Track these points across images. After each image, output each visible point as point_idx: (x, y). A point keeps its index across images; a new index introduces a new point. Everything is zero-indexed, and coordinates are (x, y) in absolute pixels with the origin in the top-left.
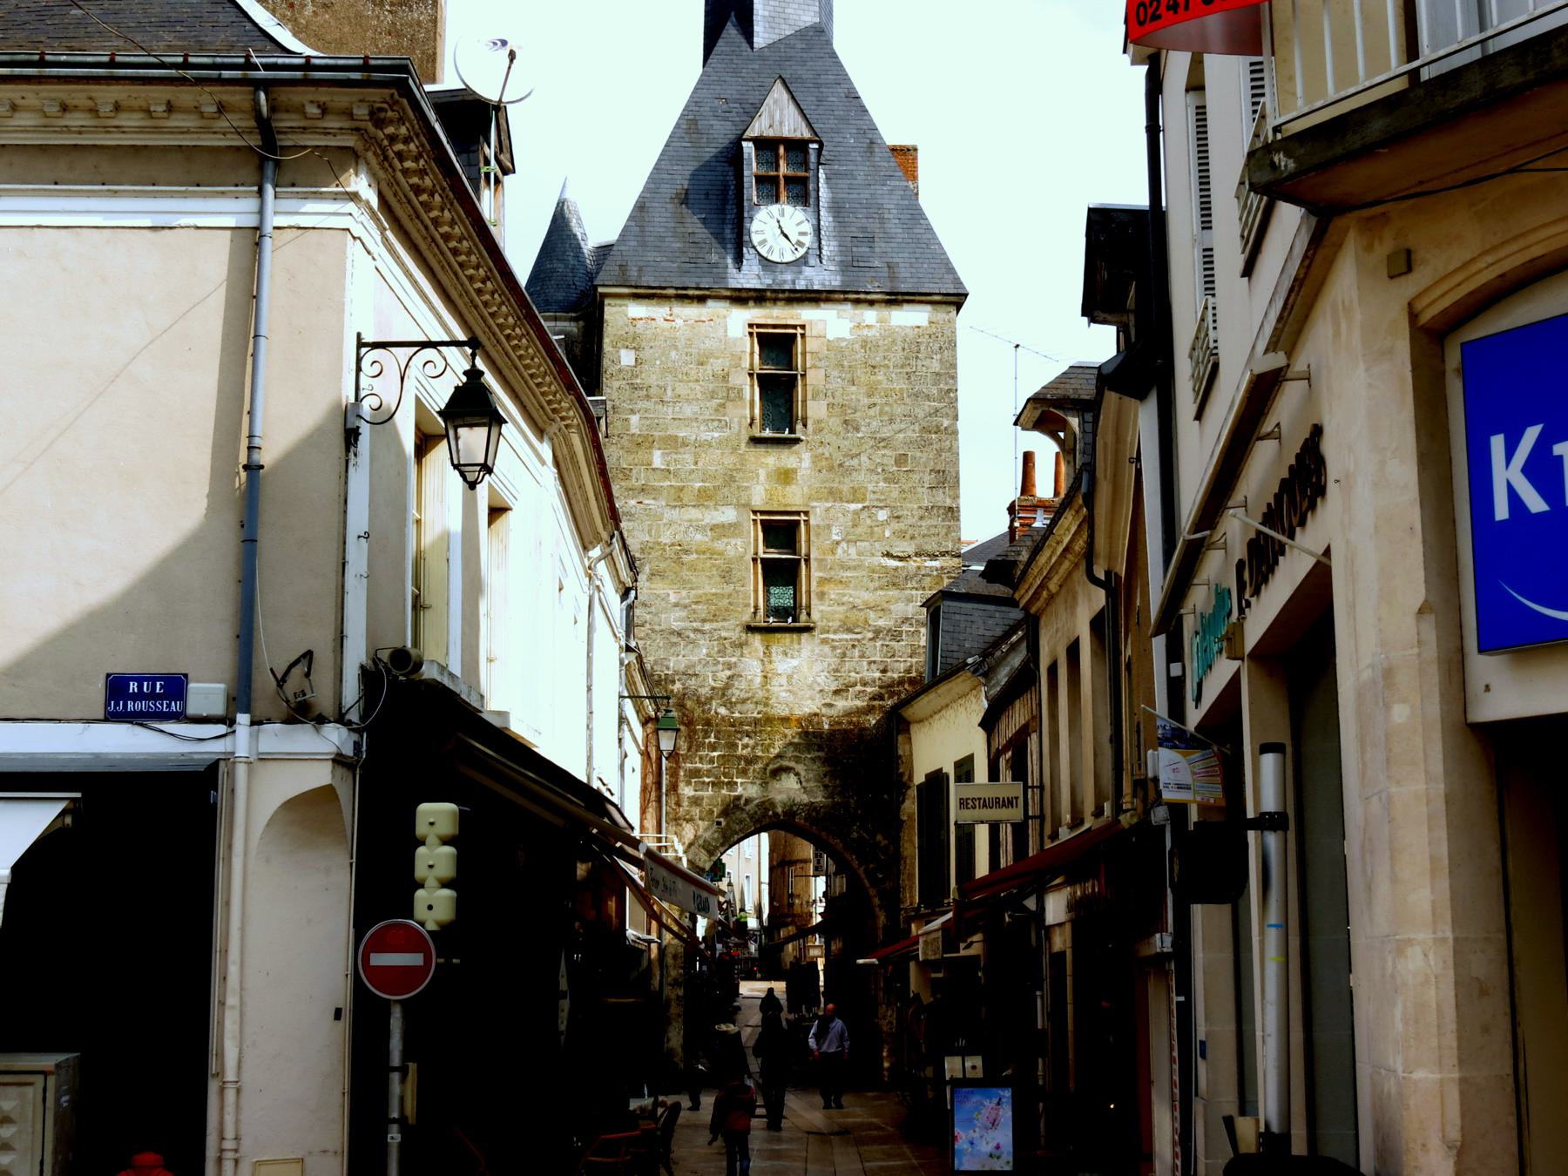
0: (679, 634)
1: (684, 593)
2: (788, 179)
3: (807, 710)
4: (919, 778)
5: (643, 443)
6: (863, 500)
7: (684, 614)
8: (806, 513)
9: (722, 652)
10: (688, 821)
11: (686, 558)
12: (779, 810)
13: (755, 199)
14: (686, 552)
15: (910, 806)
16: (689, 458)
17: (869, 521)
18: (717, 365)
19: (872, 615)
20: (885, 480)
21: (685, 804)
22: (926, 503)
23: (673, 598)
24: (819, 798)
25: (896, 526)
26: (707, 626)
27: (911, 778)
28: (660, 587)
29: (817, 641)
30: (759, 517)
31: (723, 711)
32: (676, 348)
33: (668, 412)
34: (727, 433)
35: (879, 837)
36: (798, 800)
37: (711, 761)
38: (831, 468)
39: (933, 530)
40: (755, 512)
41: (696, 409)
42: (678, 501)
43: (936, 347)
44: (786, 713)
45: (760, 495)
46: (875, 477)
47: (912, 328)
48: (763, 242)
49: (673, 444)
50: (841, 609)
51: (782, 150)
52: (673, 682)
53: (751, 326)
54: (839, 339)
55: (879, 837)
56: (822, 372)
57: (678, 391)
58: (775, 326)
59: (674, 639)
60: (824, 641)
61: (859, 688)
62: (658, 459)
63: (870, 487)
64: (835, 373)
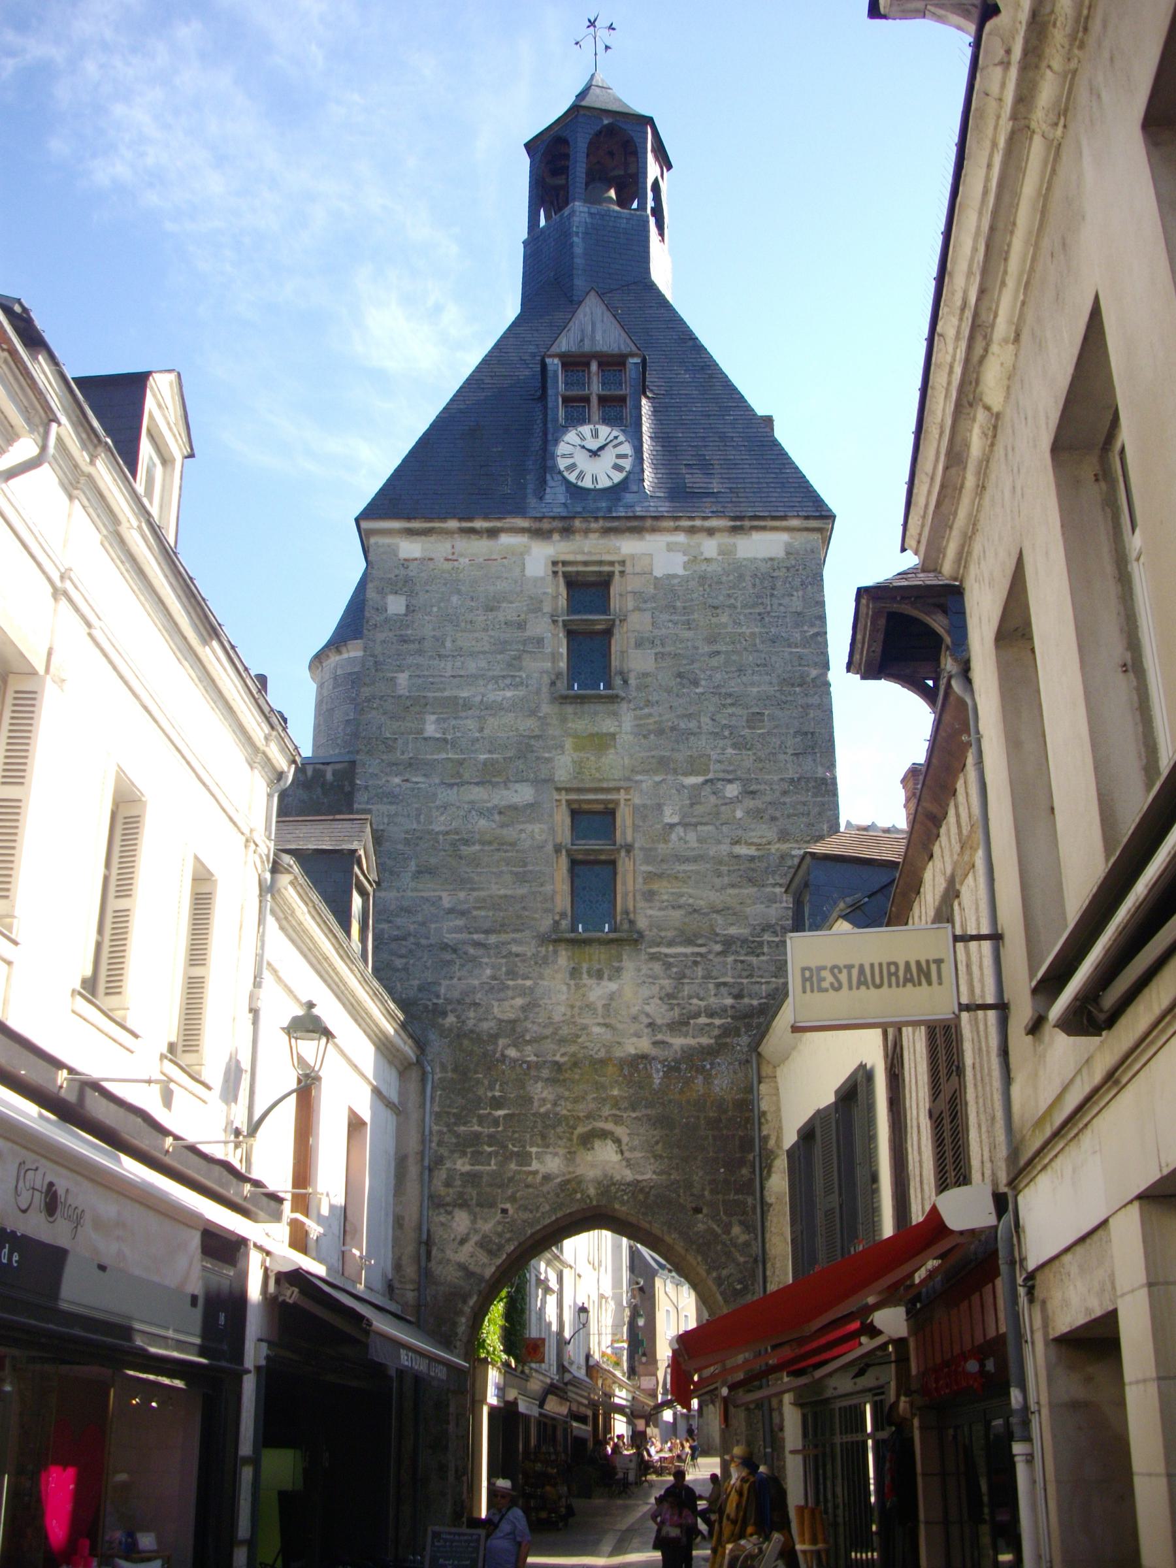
0: (455, 951)
1: (462, 895)
2: (602, 400)
3: (633, 1051)
4: (790, 1138)
5: (416, 705)
6: (706, 771)
7: (460, 922)
8: (627, 789)
9: (512, 974)
10: (461, 1206)
11: (465, 850)
12: (592, 1191)
13: (561, 421)
14: (466, 842)
15: (778, 1183)
16: (471, 724)
17: (713, 799)
18: (509, 611)
19: (720, 920)
20: (735, 746)
21: (458, 1183)
22: (790, 774)
23: (447, 902)
24: (648, 1174)
25: (750, 803)
26: (493, 939)
27: (779, 1140)
28: (429, 889)
29: (643, 957)
30: (564, 797)
31: (512, 1053)
32: (459, 592)
33: (448, 668)
34: (521, 692)
35: (736, 1230)
36: (618, 1177)
37: (496, 1122)
38: (660, 732)
39: (801, 808)
40: (558, 790)
41: (483, 664)
42: (456, 781)
43: (797, 582)
44: (602, 1054)
45: (563, 766)
46: (721, 743)
47: (766, 560)
48: (572, 467)
49: (455, 707)
50: (678, 914)
51: (594, 367)
52: (444, 1014)
53: (555, 563)
54: (670, 577)
55: (736, 1230)
56: (648, 615)
57: (459, 643)
58: (586, 563)
59: (448, 956)
60: (654, 957)
61: (703, 1020)
62: (431, 729)
63: (714, 756)
64: (665, 616)
